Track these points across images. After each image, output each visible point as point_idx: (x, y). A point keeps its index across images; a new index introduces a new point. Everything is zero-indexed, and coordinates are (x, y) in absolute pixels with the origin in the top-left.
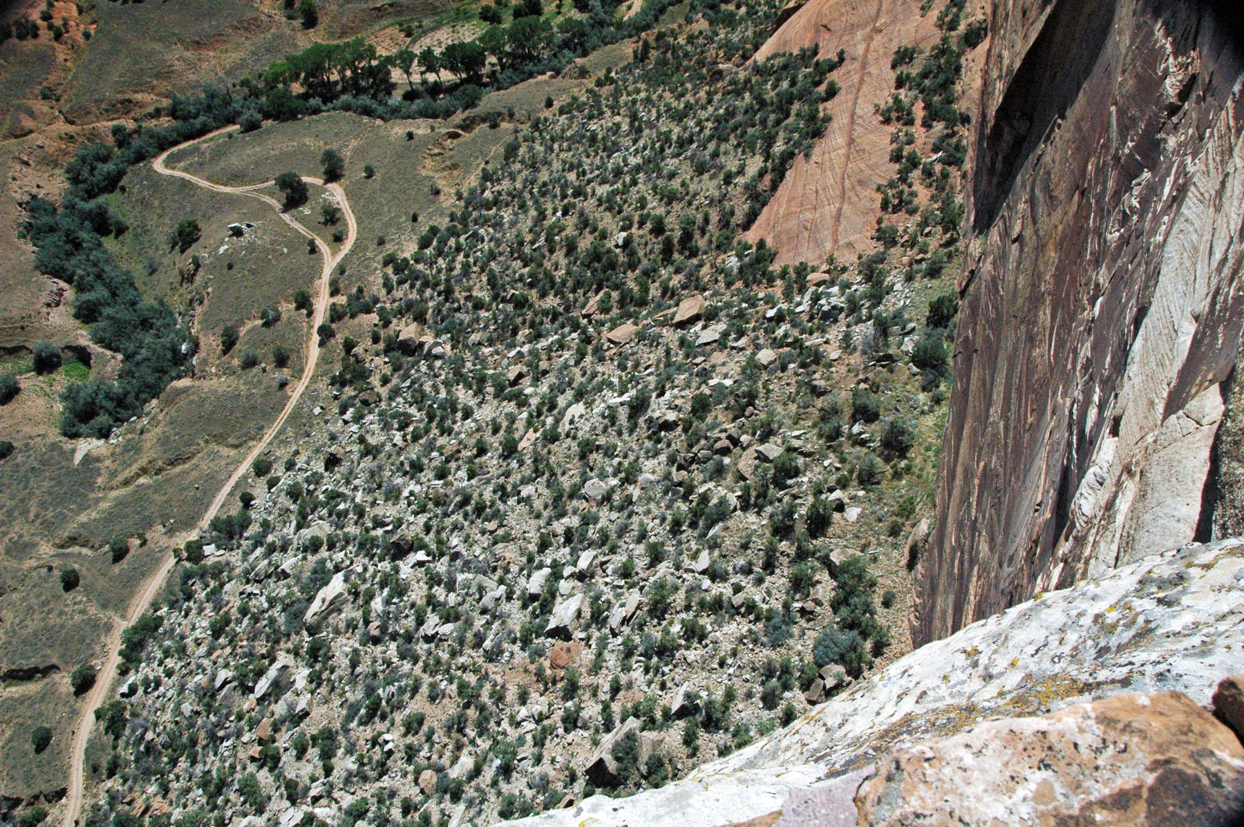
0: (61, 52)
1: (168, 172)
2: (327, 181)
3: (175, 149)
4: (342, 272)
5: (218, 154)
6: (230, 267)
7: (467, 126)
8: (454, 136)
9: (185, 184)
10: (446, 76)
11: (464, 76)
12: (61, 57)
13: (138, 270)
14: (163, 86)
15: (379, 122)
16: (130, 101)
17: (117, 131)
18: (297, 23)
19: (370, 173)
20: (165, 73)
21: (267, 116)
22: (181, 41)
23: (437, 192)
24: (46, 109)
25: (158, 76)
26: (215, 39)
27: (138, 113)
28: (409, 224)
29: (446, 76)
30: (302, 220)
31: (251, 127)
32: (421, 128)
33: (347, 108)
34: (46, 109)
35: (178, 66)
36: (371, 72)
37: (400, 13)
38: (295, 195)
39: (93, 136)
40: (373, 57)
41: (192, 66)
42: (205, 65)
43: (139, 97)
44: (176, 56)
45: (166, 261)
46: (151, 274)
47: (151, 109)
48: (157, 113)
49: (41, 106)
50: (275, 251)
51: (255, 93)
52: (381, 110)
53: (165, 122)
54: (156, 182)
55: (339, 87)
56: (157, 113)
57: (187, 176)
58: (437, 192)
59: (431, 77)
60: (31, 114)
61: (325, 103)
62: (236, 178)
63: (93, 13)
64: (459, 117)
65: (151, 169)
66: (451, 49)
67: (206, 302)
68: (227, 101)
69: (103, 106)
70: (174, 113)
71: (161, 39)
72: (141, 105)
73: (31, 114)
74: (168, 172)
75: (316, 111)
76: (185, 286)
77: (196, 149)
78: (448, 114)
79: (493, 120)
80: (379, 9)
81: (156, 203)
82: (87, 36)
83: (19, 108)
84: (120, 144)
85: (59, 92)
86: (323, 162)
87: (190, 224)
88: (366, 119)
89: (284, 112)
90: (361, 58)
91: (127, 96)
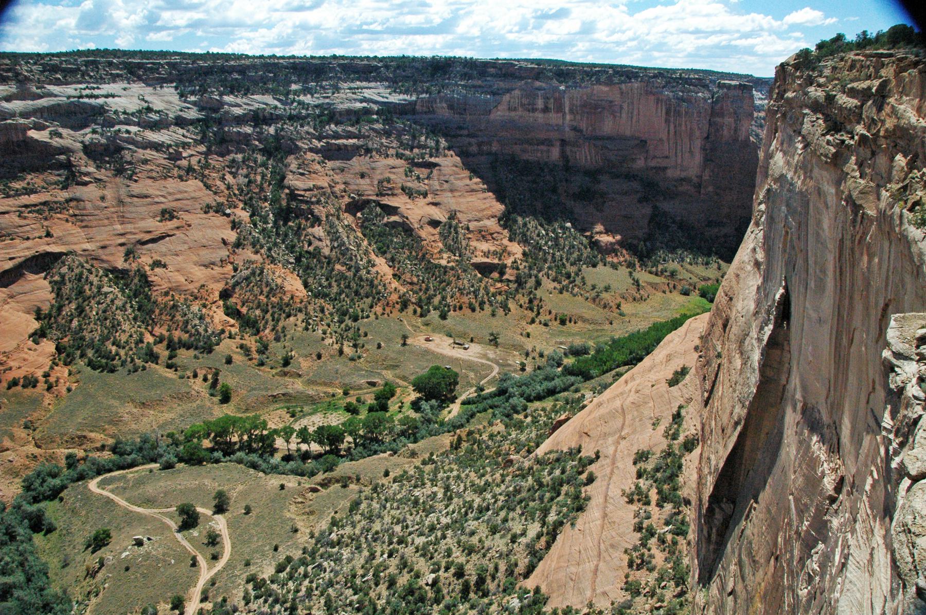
0: (48, 398)
1: (99, 491)
2: (215, 513)
3: (108, 475)
4: (213, 584)
5: (140, 482)
6: (127, 569)
7: (325, 484)
8: (314, 490)
9: (109, 501)
10: (315, 447)
11: (328, 448)
12: (47, 401)
13: (54, 563)
14: (112, 430)
15: (261, 474)
16: (85, 437)
17: (69, 457)
18: (216, 399)
19: (248, 511)
20: (115, 421)
21: (181, 460)
22: (133, 401)
23: (296, 531)
24: (23, 435)
25: (111, 422)
26: (158, 403)
27: (88, 446)
28: (271, 552)
29: (315, 447)
30: (191, 540)
31: (168, 466)
32: (292, 482)
33: (240, 461)
34: (23, 435)
35: (126, 417)
36: (262, 438)
37: (288, 401)
38: (189, 520)
39: (52, 458)
40: (265, 428)
41: (136, 419)
42: (145, 419)
43: (92, 435)
44: (127, 411)
45: (79, 558)
46: (63, 567)
47: (98, 445)
48: (103, 448)
49: (21, 433)
50: (165, 561)
51: (176, 443)
52: (264, 466)
53: (107, 455)
54: (88, 497)
55: (237, 447)
56: (103, 448)
57: (112, 496)
58: (296, 531)
59: (304, 447)
60: (12, 437)
61: (224, 456)
62: (149, 502)
63: (78, 376)
64: (320, 477)
65: (86, 487)
66: (321, 429)
67: (101, 595)
68: (154, 447)
69: (65, 438)
70: (114, 450)
71: (120, 398)
72: (92, 441)
73: (12, 437)
74: (99, 491)
75: (217, 461)
76: (88, 580)
77: (124, 477)
78: (312, 474)
79: (345, 482)
80: (274, 397)
81: (84, 513)
82: (69, 390)
83: (5, 433)
84: (69, 466)
85: (36, 425)
86: (215, 498)
87: (105, 532)
88: (252, 471)
89: (193, 459)
90: (256, 427)
91: (84, 434)
